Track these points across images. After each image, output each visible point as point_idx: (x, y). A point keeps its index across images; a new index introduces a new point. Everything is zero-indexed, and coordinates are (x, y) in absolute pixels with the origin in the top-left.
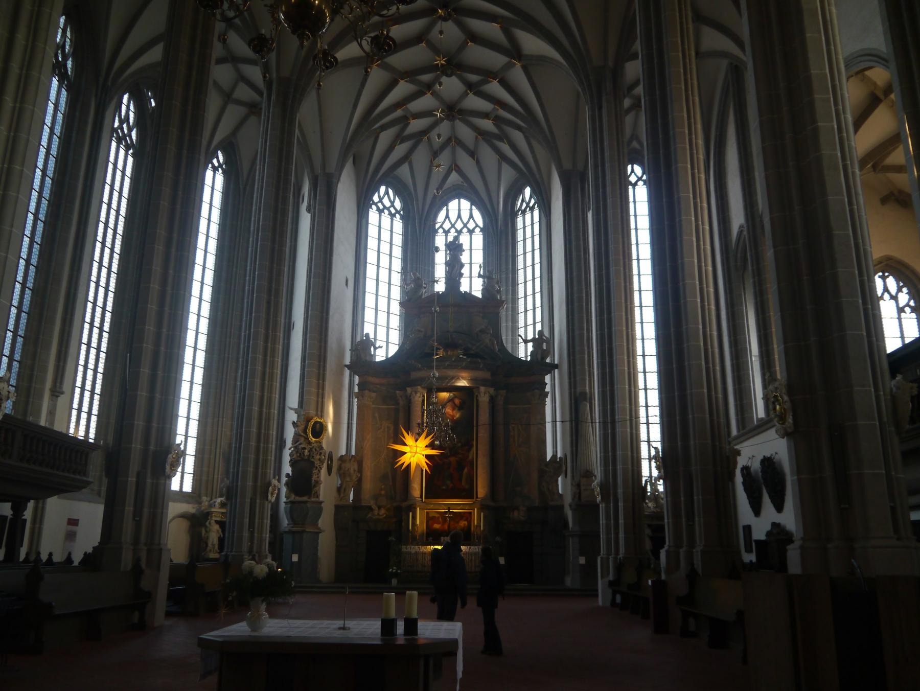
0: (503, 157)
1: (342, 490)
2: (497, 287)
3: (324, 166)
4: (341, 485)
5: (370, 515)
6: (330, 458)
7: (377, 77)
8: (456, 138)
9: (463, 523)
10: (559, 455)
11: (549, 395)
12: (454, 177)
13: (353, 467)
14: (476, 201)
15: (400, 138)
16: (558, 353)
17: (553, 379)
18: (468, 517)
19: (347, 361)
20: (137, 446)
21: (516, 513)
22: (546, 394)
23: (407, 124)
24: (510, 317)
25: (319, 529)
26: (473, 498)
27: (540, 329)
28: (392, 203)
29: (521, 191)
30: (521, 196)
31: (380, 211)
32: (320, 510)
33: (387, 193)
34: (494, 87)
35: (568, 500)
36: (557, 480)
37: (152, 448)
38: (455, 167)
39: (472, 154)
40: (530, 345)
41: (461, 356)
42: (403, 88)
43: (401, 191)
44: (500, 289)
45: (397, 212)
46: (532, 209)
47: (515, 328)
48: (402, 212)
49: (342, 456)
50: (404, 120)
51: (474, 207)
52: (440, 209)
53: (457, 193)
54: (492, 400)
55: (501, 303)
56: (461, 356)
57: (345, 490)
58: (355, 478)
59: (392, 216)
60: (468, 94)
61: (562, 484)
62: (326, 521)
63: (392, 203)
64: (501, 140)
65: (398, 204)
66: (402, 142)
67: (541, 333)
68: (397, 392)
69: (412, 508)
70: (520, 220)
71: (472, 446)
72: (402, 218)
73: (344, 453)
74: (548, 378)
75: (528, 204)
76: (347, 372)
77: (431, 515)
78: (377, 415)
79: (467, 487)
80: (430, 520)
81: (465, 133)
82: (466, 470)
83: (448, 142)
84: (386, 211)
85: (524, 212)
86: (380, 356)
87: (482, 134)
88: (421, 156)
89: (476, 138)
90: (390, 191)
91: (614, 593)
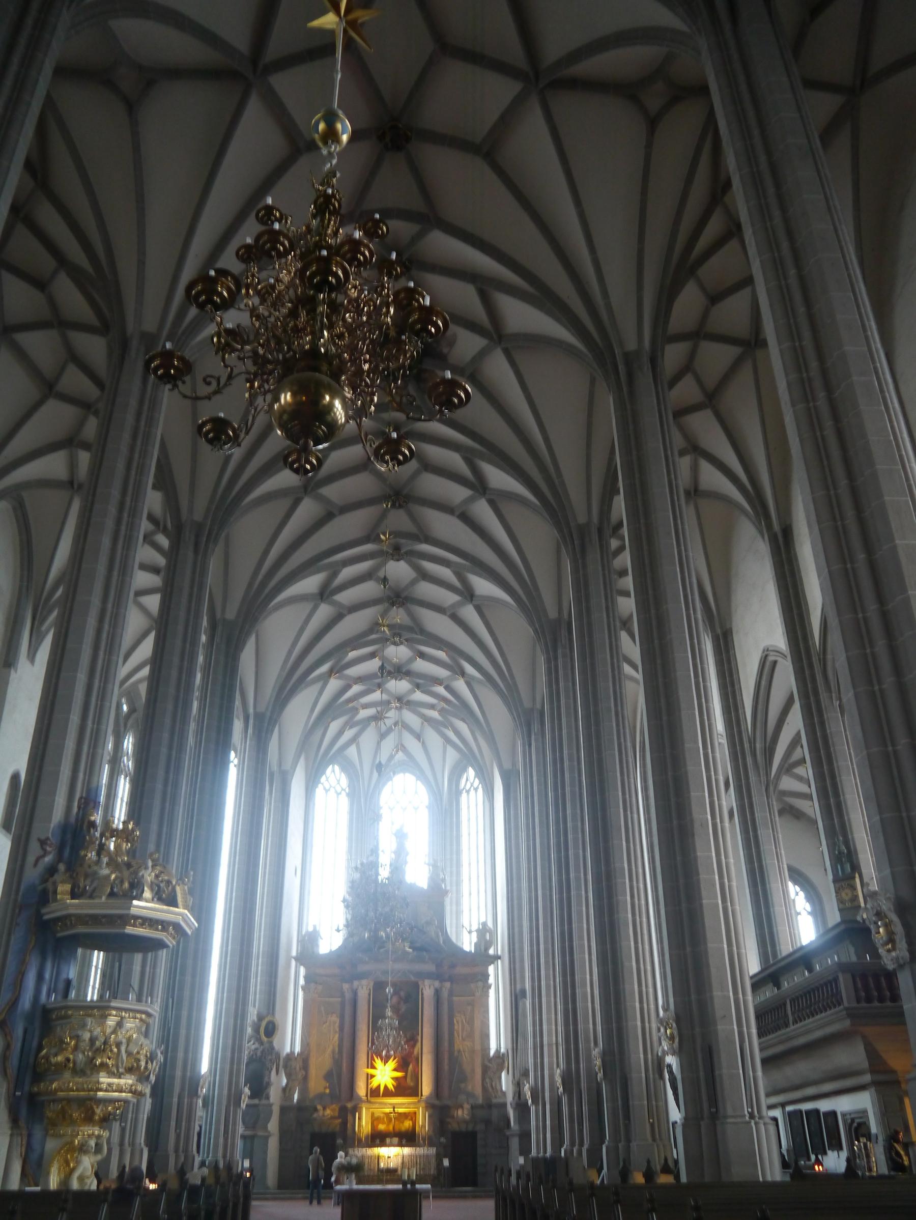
0: (448, 740)
1: (287, 1091)
2: (442, 876)
3: (280, 764)
4: (287, 1085)
5: (315, 1115)
7: (334, 684)
8: (403, 722)
9: (407, 1124)
10: (503, 1050)
11: (493, 987)
12: (400, 755)
13: (298, 1065)
14: (421, 775)
15: (349, 724)
16: (500, 946)
17: (496, 969)
18: (412, 1116)
19: (294, 953)
20: (178, 1073)
21: (460, 1112)
22: (490, 987)
23: (358, 713)
24: (454, 900)
25: (269, 1132)
26: (418, 1096)
27: (484, 920)
28: (339, 781)
29: (464, 770)
30: (466, 774)
31: (327, 791)
32: (271, 1113)
33: (333, 771)
34: (441, 690)
35: (510, 1098)
36: (500, 1078)
37: (188, 1074)
38: (401, 747)
39: (418, 737)
40: (474, 935)
41: (407, 949)
42: (356, 689)
43: (348, 768)
44: (445, 877)
45: (343, 789)
46: (476, 789)
47: (459, 913)
48: (347, 790)
49: (288, 1055)
50: (355, 711)
51: (418, 782)
52: (385, 784)
53: (403, 767)
54: (437, 993)
55: (446, 892)
56: (407, 949)
57: (290, 1090)
58: (300, 1076)
59: (338, 794)
60: (415, 691)
61: (505, 1082)
62: (273, 1126)
63: (339, 781)
64: (446, 727)
65: (344, 781)
66: (351, 727)
67: (484, 924)
68: (344, 984)
69: (356, 1109)
70: (464, 797)
71: (416, 1041)
72: (348, 795)
73: (288, 1050)
74: (491, 969)
75: (472, 785)
76: (293, 963)
77: (376, 1115)
78: (322, 1009)
79: (412, 1084)
80: (375, 1120)
81: (410, 717)
82: (411, 1067)
83: (396, 724)
84: (332, 790)
85: (468, 792)
87: (427, 719)
88: (369, 737)
89: (423, 723)
90: (337, 768)
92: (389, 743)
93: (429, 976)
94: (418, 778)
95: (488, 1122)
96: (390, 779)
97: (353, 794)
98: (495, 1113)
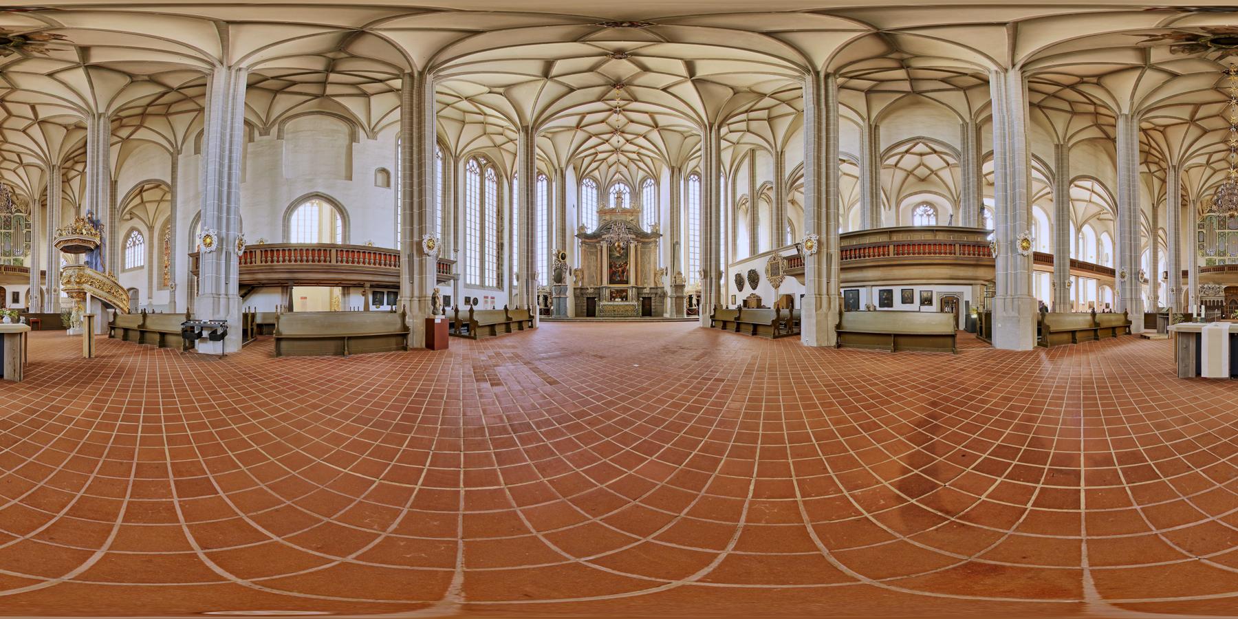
6: (571, 270)
16: (664, 228)
62: (570, 293)
76: (576, 238)
81: (623, 159)
86: (589, 232)
88: (604, 166)
91: (713, 321)
92: (613, 168)
93: (633, 239)
94: (625, 185)
95: (656, 294)
96: (614, 185)
97: (598, 188)
98: (659, 291)
